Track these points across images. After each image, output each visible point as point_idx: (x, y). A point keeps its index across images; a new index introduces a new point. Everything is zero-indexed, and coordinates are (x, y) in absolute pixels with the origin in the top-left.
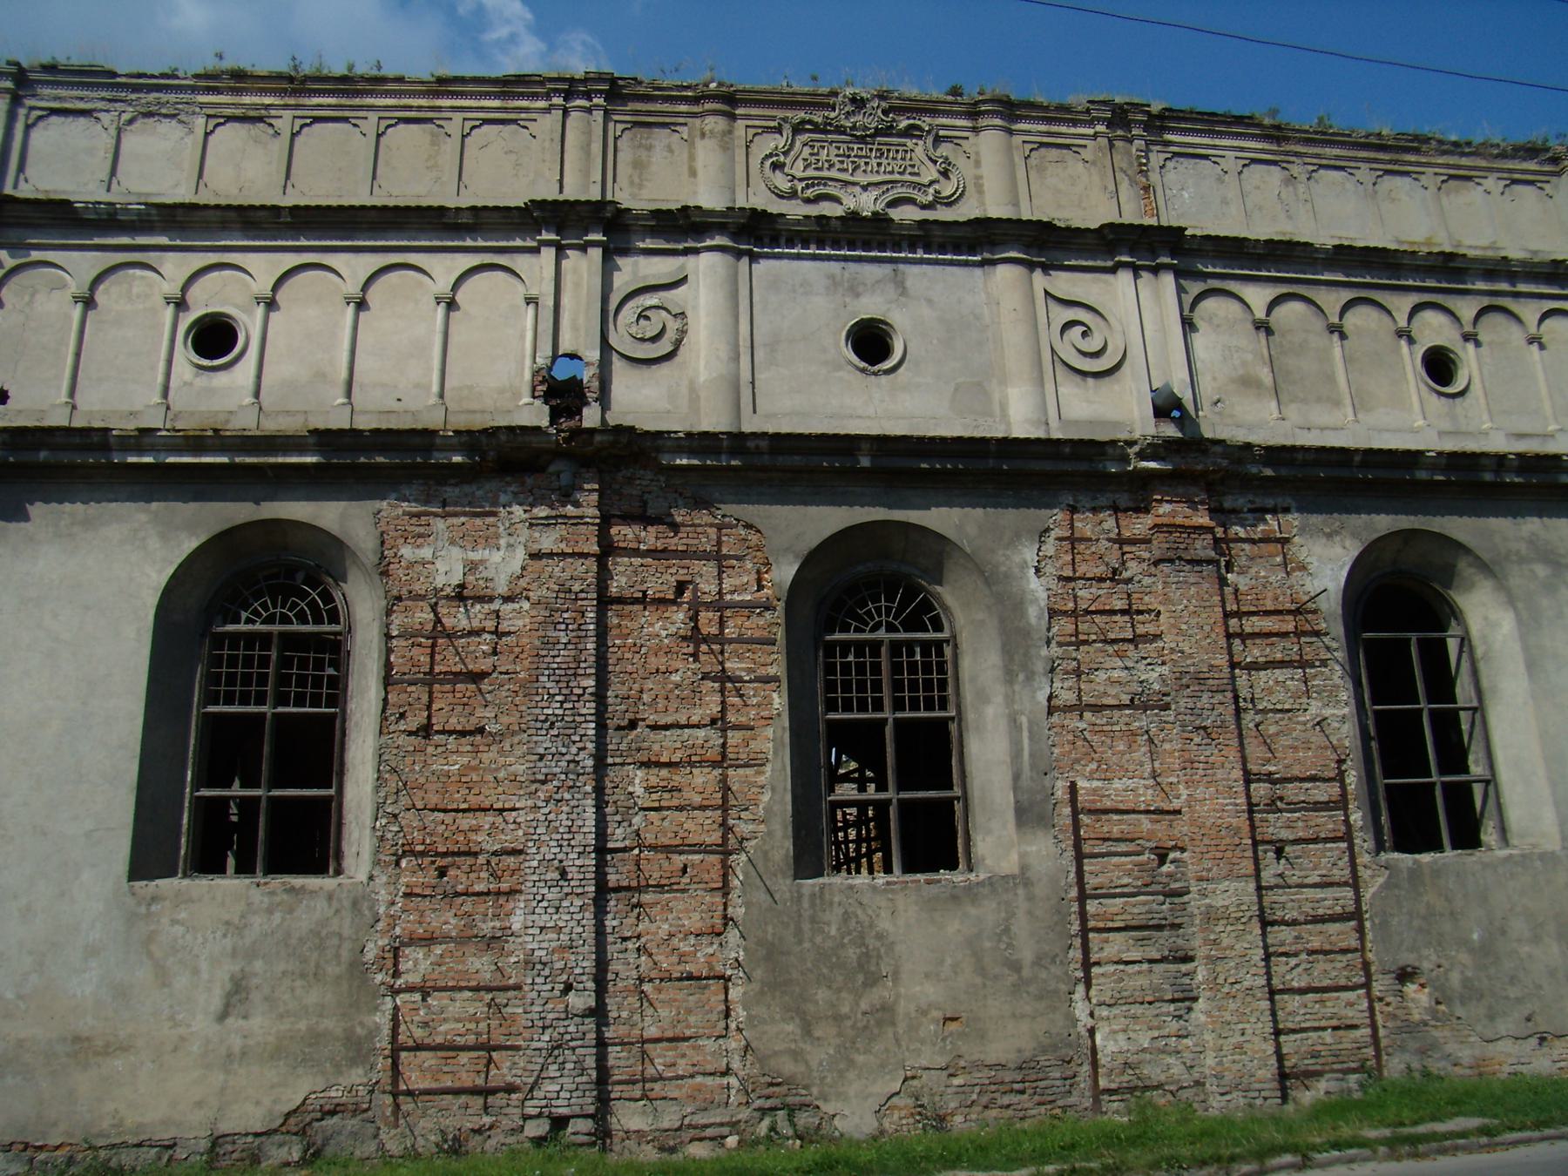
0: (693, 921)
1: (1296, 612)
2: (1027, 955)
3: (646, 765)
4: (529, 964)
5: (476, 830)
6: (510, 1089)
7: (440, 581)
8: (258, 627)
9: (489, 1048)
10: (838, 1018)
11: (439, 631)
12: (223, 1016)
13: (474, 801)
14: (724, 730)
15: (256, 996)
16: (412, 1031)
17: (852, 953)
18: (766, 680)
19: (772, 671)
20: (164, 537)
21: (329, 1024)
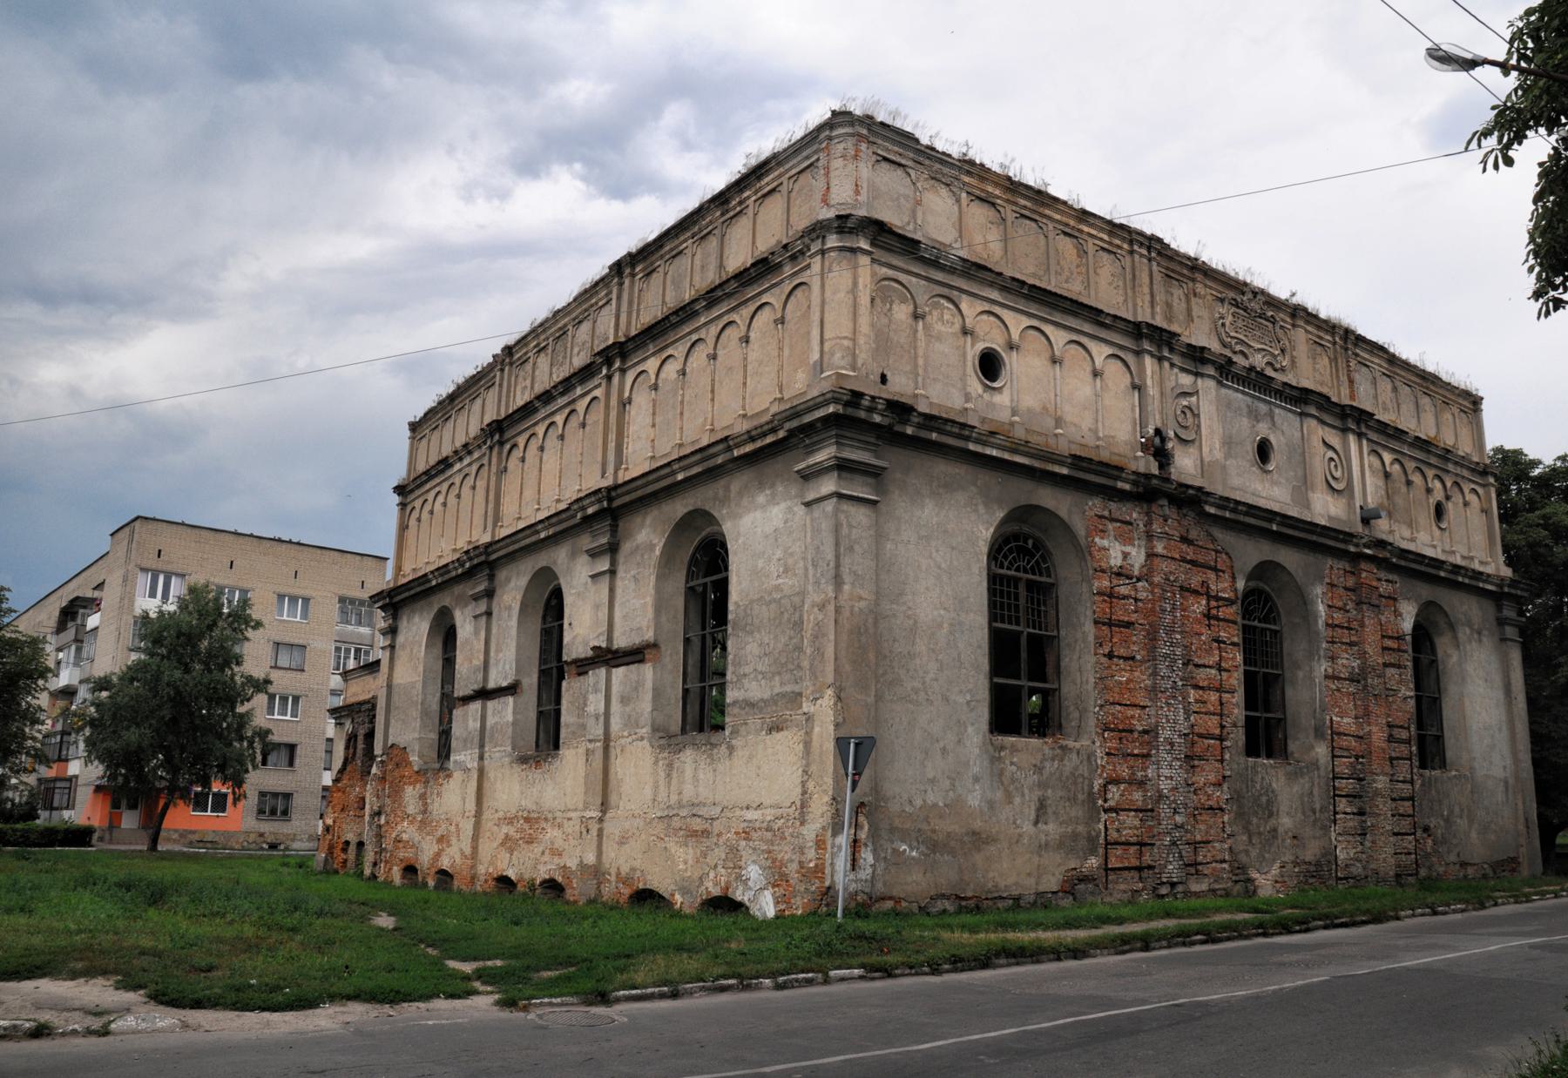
0: (1212, 777)
1: (1398, 638)
2: (1317, 806)
3: (1196, 687)
4: (1161, 796)
5: (1133, 717)
6: (1150, 867)
7: (1112, 562)
8: (1012, 573)
9: (1141, 844)
10: (1260, 834)
11: (1111, 595)
12: (1036, 823)
13: (1134, 700)
14: (1220, 669)
15: (1050, 811)
16: (1113, 835)
17: (1264, 799)
18: (1233, 644)
19: (1236, 640)
20: (986, 505)
21: (1080, 828)
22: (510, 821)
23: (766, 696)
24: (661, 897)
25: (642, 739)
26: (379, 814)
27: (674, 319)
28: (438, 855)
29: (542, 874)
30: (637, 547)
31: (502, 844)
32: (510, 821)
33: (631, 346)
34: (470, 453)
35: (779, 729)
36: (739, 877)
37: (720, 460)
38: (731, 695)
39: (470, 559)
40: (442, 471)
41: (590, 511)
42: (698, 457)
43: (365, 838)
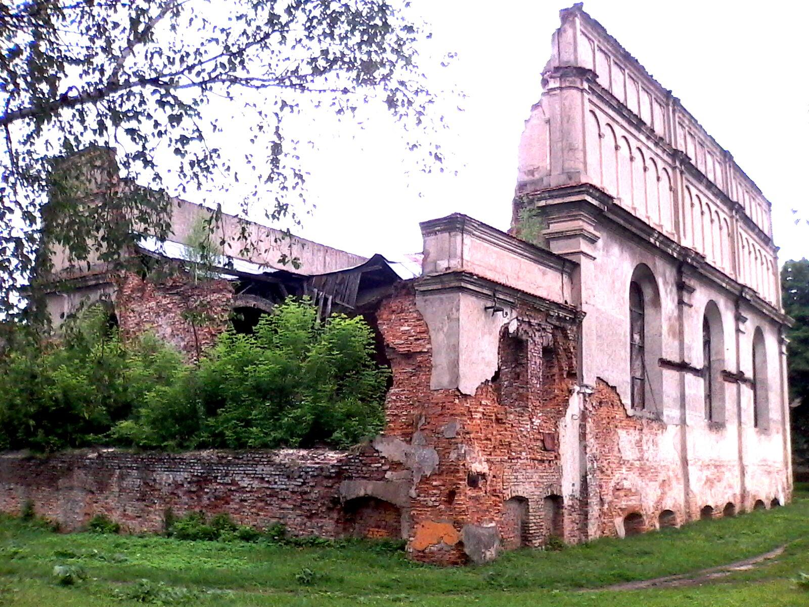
34: (656, 144)
39: (693, 259)
40: (630, 123)
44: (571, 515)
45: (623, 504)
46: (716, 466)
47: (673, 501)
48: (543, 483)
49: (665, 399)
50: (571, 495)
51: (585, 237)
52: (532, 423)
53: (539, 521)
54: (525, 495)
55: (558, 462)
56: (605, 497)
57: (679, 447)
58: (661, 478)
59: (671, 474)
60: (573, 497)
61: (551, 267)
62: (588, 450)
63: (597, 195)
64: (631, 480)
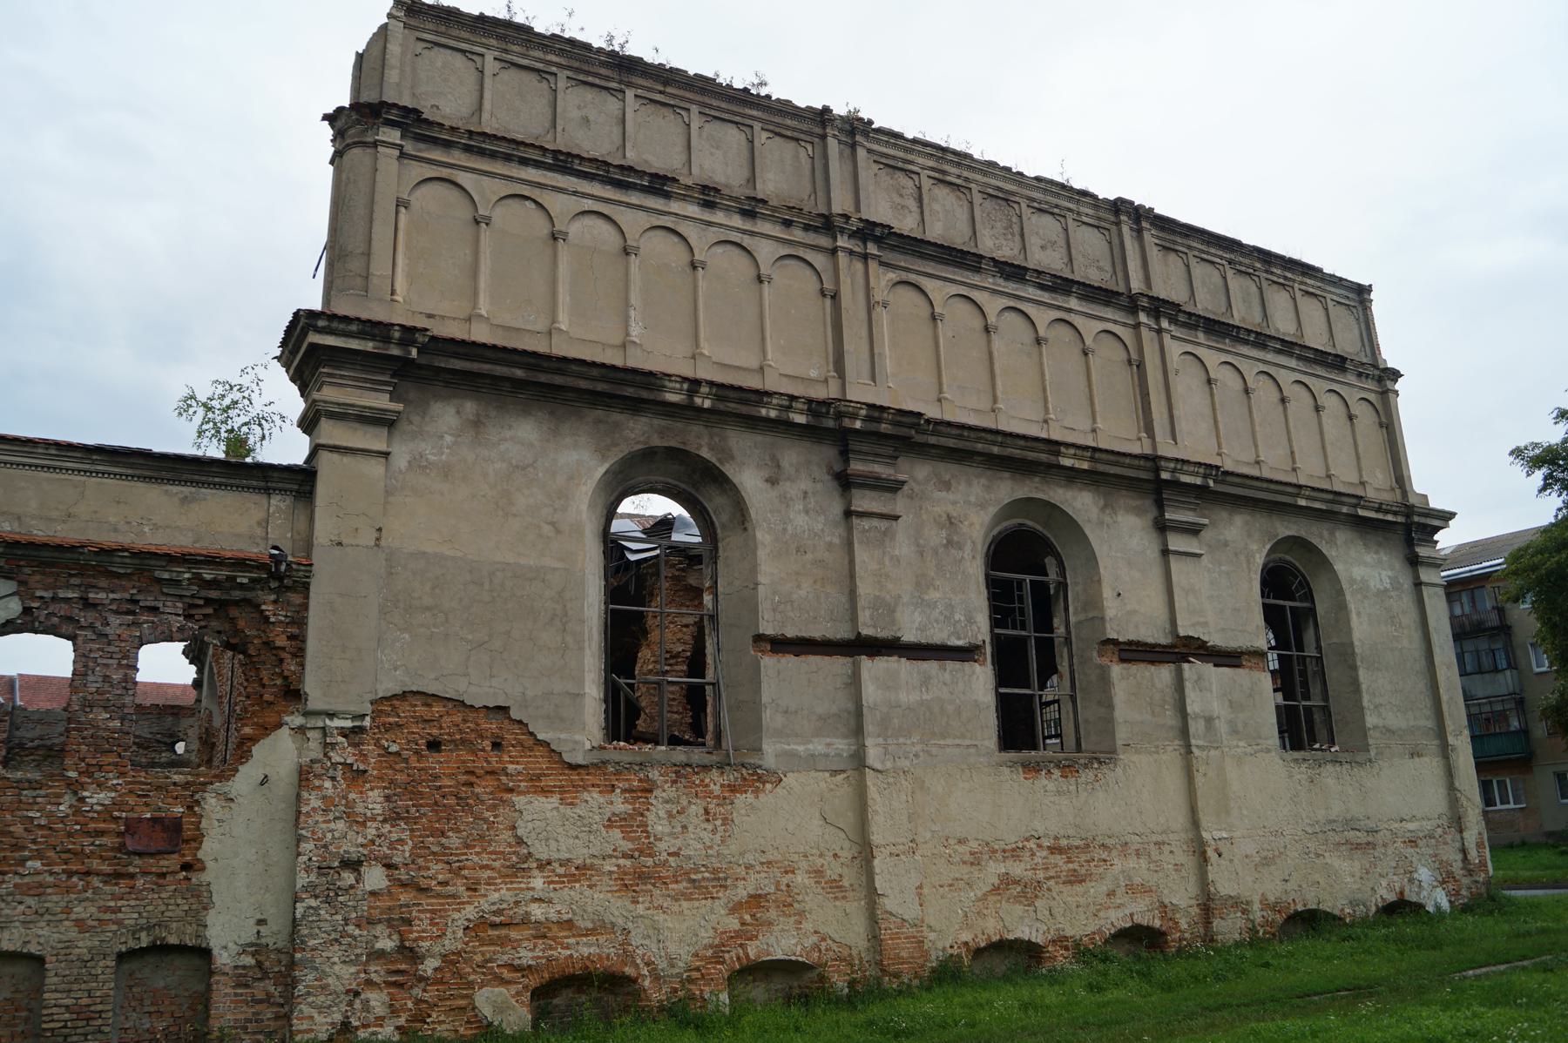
22: (1014, 853)
23: (1404, 725)
24: (1334, 917)
25: (1268, 751)
26: (353, 865)
27: (1182, 318)
28: (743, 936)
29: (1117, 919)
30: (1226, 544)
31: (996, 890)
32: (1014, 853)
33: (1182, 318)
35: (1420, 755)
36: (1411, 880)
37: (1345, 510)
38: (1371, 720)
41: (1185, 479)
42: (1330, 497)
43: (227, 934)
44: (247, 986)
45: (526, 956)
46: (1053, 850)
47: (815, 938)
48: (119, 923)
49: (770, 718)
50: (252, 945)
51: (332, 416)
52: (82, 800)
53: (85, 1001)
54: (33, 949)
55: (195, 878)
56: (426, 944)
57: (848, 820)
58: (742, 892)
59: (800, 879)
60: (257, 949)
61: (210, 485)
62: (307, 846)
63: (354, 328)
64: (600, 900)
